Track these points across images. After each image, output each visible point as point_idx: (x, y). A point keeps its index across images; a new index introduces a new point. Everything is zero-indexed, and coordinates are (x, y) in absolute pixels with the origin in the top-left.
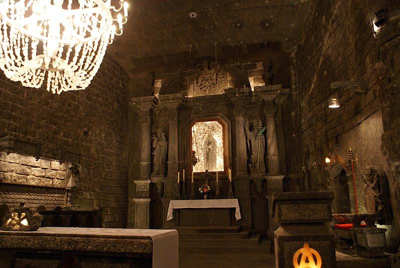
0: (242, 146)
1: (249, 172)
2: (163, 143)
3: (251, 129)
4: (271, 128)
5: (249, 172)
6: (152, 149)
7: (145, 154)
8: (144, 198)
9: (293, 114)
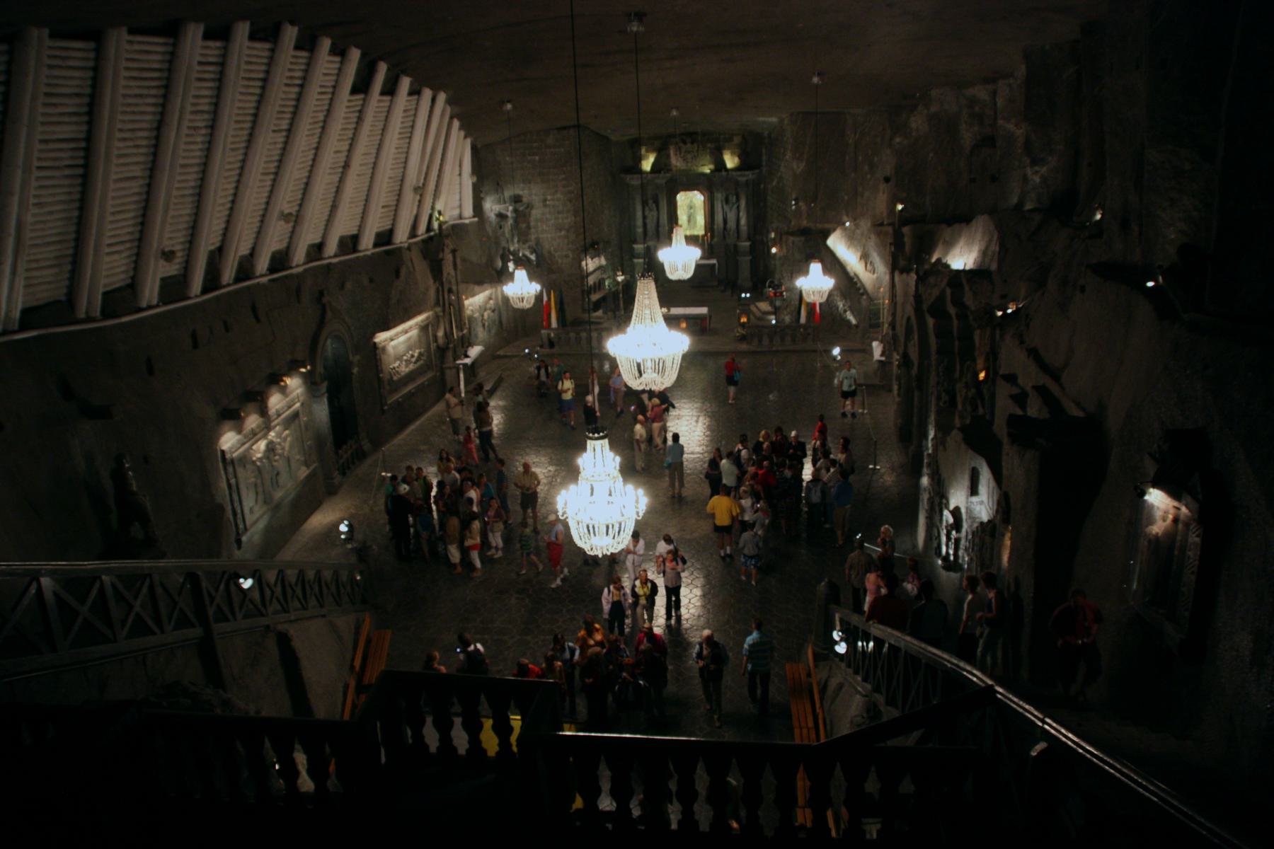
0: (719, 218)
1: (724, 237)
2: (655, 213)
3: (727, 201)
4: (743, 203)
5: (724, 237)
6: (644, 217)
7: (639, 222)
8: (642, 258)
9: (762, 186)
